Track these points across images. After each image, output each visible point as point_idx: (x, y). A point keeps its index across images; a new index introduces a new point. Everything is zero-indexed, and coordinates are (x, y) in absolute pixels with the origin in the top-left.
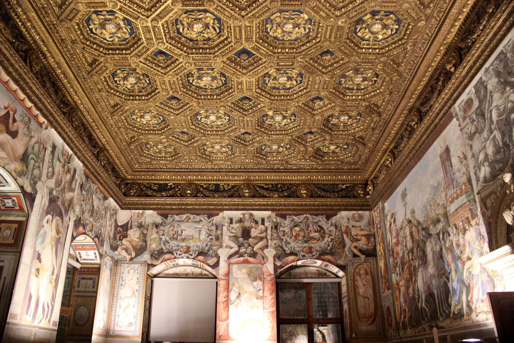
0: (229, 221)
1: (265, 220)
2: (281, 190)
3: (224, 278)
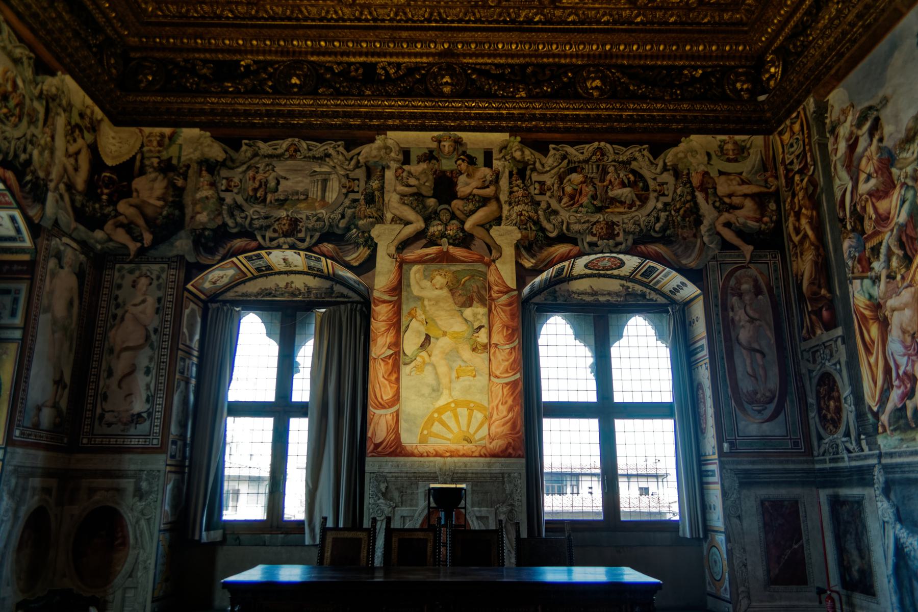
0: (401, 157)
1: (495, 156)
2: (533, 80)
3: (386, 297)
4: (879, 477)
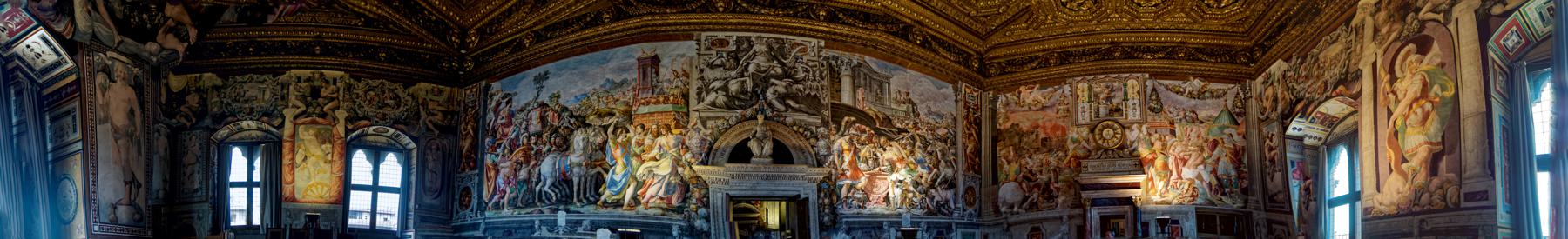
4: (483, 227)
